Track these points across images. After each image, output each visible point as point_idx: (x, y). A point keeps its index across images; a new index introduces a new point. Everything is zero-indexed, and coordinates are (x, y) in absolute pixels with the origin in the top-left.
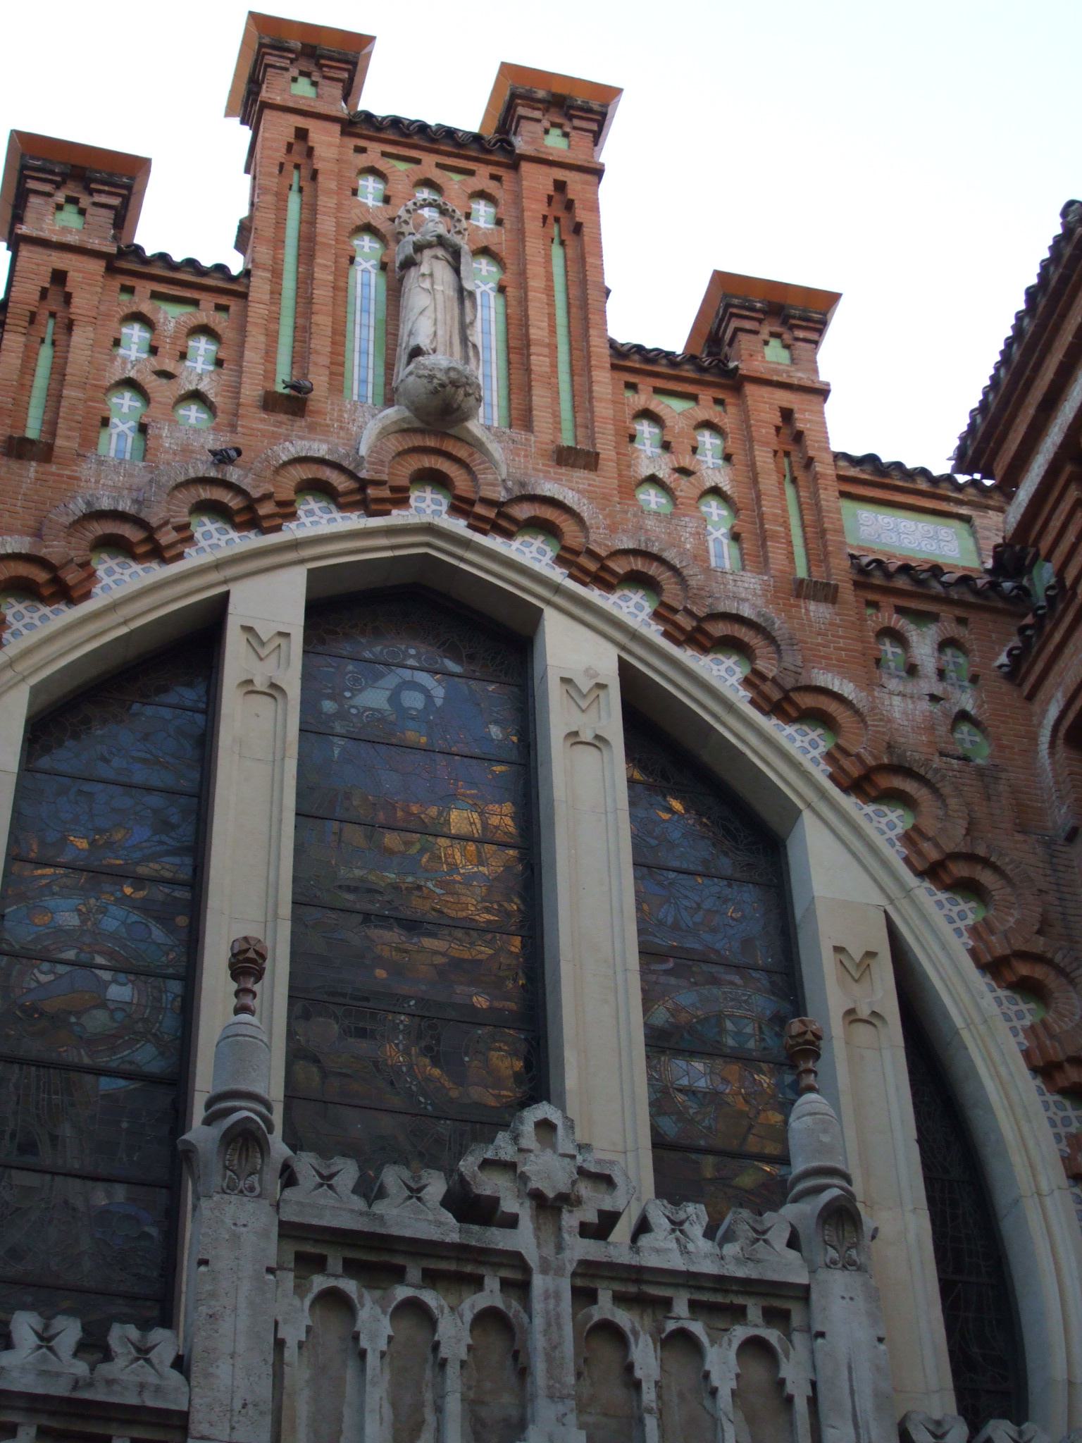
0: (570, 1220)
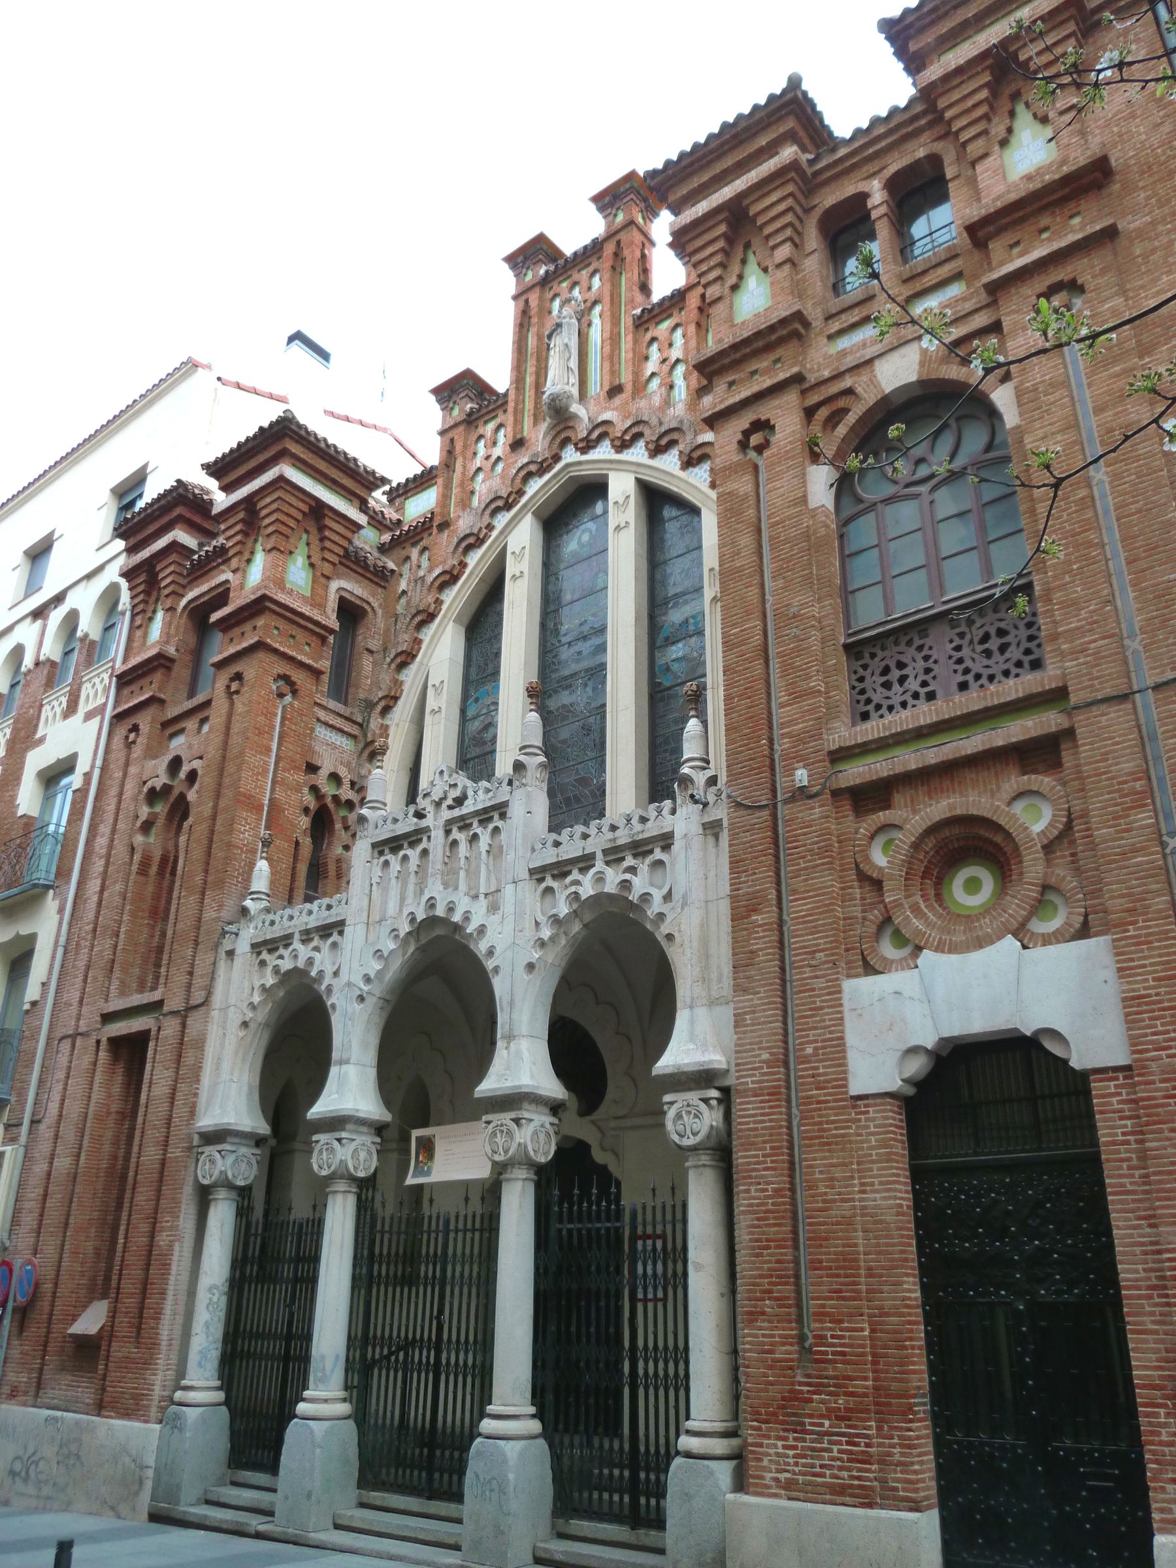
0: (444, 806)
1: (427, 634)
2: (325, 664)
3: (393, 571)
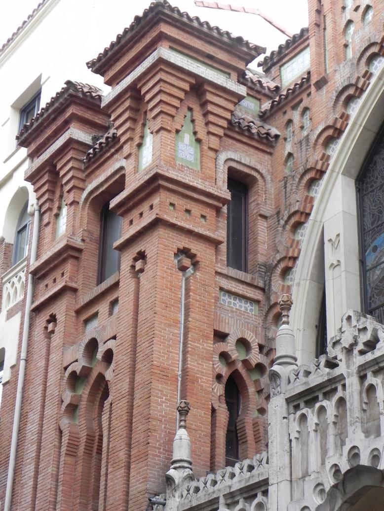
0: (356, 352)
1: (318, 191)
2: (221, 234)
3: (277, 136)
